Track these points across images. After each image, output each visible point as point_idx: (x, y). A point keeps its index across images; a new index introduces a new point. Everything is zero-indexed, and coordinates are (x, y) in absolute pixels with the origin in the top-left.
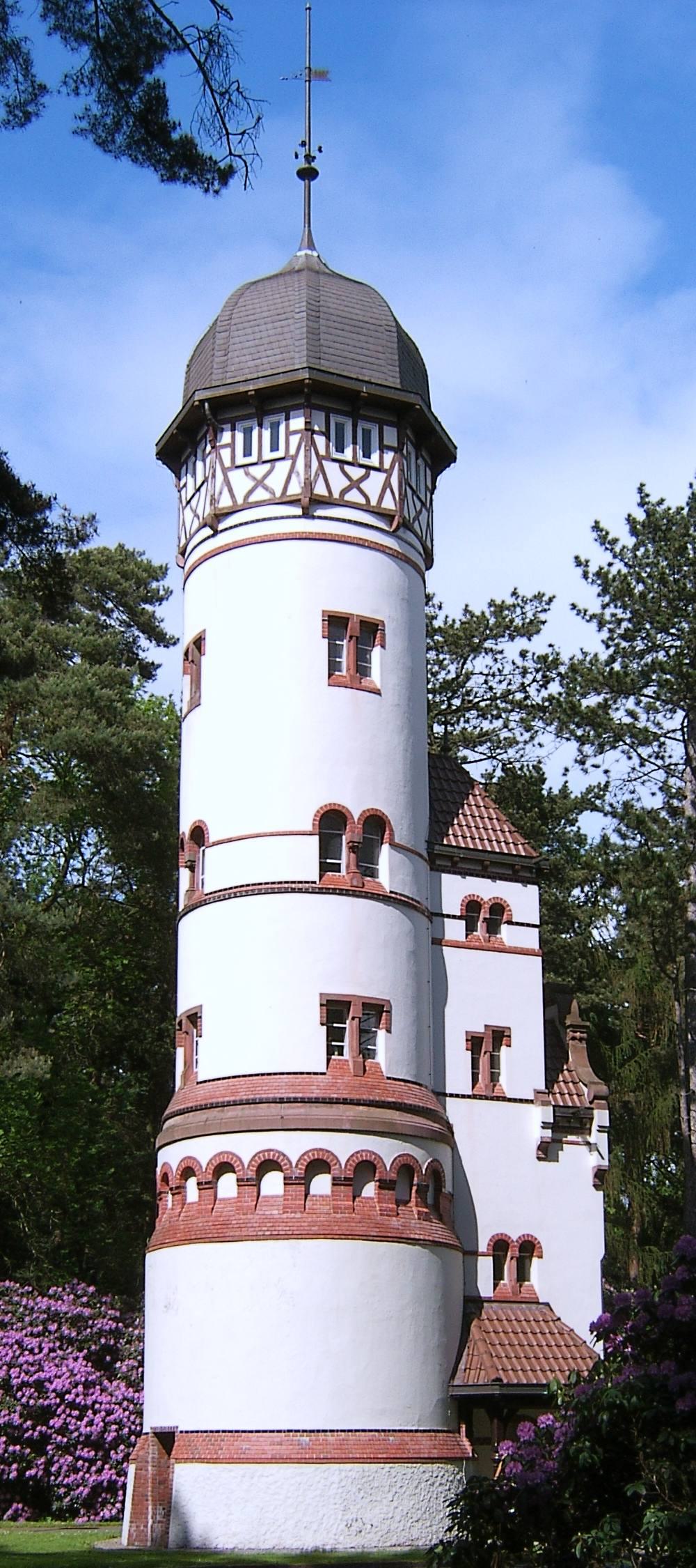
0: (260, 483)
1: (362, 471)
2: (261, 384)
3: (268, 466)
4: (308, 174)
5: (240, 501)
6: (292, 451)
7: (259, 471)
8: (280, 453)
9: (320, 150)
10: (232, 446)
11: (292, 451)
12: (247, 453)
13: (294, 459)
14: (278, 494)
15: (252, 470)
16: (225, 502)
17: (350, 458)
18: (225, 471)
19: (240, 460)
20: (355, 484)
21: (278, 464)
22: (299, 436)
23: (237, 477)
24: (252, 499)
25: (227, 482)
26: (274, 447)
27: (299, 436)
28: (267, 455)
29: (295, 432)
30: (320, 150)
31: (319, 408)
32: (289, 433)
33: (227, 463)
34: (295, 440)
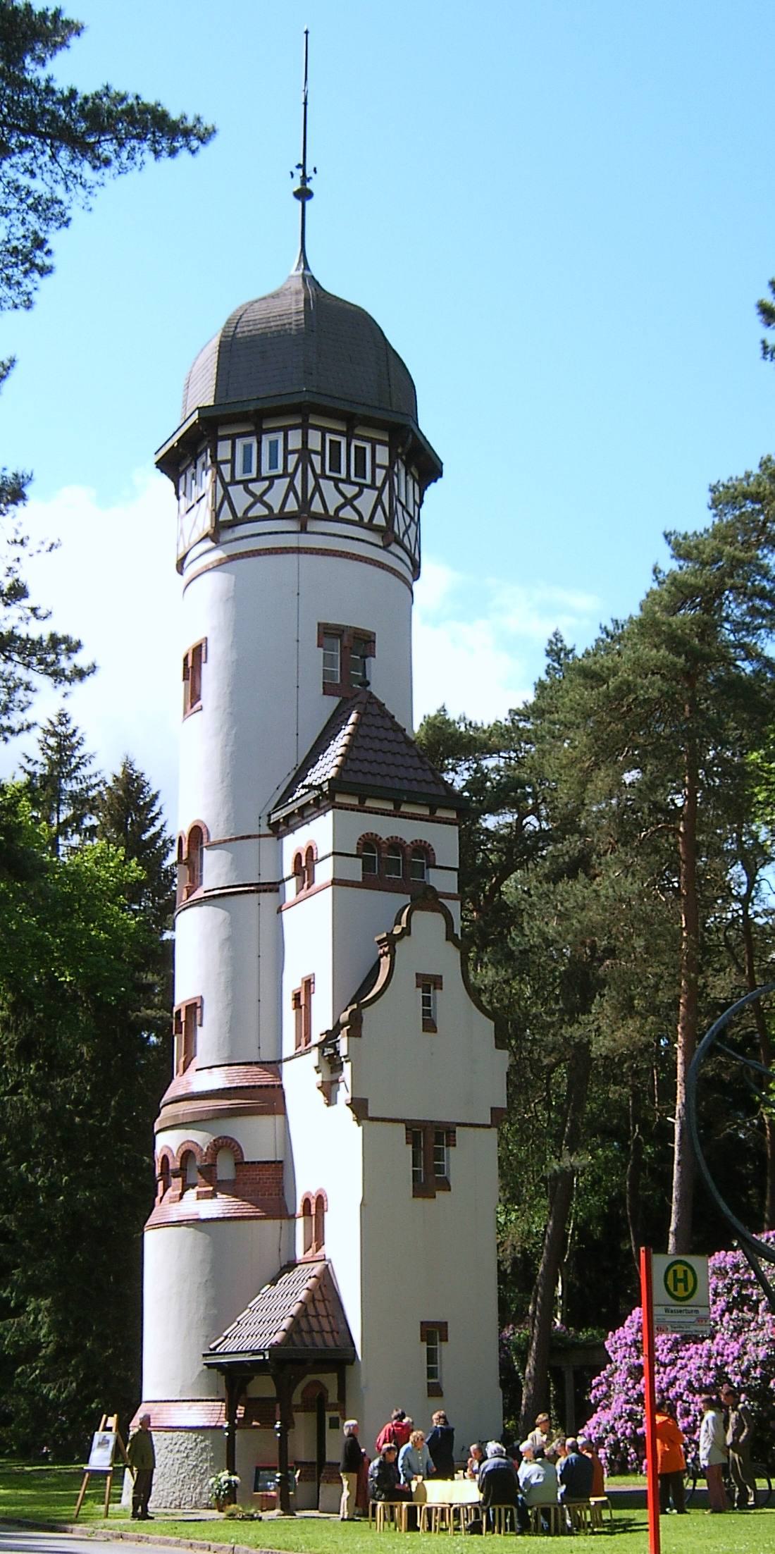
0: (259, 499)
1: (357, 489)
2: (259, 405)
3: (267, 483)
4: (304, 195)
6: (290, 470)
7: (258, 488)
8: (280, 471)
9: (315, 170)
10: (232, 461)
11: (290, 470)
12: (247, 469)
13: (293, 476)
14: (276, 511)
15: (251, 486)
17: (343, 475)
19: (239, 477)
20: (349, 502)
22: (296, 456)
24: (250, 515)
26: (273, 465)
27: (296, 456)
28: (266, 472)
29: (293, 452)
30: (315, 170)
31: (316, 428)
33: (228, 479)
34: (292, 459)
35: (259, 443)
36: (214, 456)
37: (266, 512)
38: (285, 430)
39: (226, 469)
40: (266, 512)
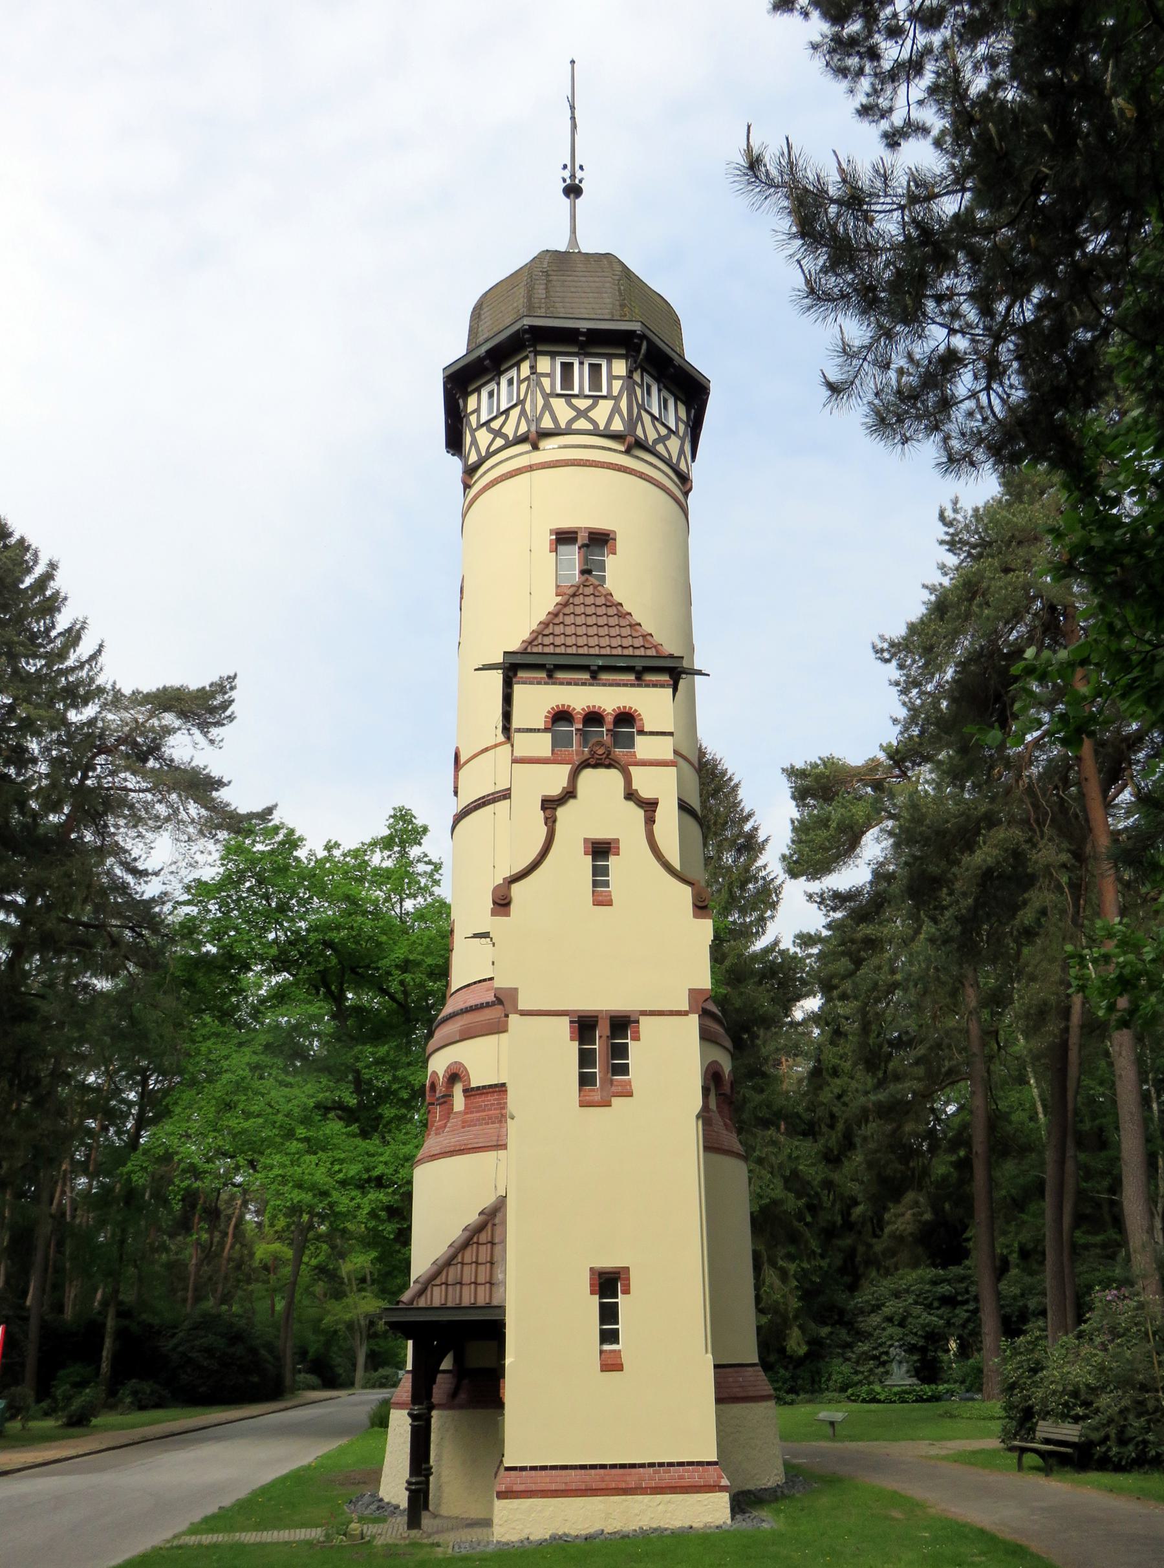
0: (582, 414)
3: (590, 402)
5: (563, 426)
6: (615, 393)
7: (582, 404)
11: (615, 393)
13: (617, 399)
14: (602, 428)
15: (574, 401)
16: (547, 423)
17: (576, 391)
18: (546, 397)
21: (601, 402)
23: (558, 404)
24: (575, 426)
25: (547, 406)
29: (618, 378)
32: (611, 377)
35: (581, 363)
36: (533, 368)
37: (590, 427)
38: (610, 357)
39: (546, 382)
40: (590, 427)
